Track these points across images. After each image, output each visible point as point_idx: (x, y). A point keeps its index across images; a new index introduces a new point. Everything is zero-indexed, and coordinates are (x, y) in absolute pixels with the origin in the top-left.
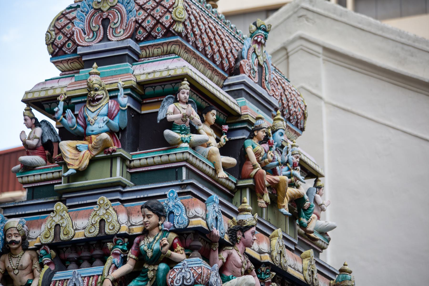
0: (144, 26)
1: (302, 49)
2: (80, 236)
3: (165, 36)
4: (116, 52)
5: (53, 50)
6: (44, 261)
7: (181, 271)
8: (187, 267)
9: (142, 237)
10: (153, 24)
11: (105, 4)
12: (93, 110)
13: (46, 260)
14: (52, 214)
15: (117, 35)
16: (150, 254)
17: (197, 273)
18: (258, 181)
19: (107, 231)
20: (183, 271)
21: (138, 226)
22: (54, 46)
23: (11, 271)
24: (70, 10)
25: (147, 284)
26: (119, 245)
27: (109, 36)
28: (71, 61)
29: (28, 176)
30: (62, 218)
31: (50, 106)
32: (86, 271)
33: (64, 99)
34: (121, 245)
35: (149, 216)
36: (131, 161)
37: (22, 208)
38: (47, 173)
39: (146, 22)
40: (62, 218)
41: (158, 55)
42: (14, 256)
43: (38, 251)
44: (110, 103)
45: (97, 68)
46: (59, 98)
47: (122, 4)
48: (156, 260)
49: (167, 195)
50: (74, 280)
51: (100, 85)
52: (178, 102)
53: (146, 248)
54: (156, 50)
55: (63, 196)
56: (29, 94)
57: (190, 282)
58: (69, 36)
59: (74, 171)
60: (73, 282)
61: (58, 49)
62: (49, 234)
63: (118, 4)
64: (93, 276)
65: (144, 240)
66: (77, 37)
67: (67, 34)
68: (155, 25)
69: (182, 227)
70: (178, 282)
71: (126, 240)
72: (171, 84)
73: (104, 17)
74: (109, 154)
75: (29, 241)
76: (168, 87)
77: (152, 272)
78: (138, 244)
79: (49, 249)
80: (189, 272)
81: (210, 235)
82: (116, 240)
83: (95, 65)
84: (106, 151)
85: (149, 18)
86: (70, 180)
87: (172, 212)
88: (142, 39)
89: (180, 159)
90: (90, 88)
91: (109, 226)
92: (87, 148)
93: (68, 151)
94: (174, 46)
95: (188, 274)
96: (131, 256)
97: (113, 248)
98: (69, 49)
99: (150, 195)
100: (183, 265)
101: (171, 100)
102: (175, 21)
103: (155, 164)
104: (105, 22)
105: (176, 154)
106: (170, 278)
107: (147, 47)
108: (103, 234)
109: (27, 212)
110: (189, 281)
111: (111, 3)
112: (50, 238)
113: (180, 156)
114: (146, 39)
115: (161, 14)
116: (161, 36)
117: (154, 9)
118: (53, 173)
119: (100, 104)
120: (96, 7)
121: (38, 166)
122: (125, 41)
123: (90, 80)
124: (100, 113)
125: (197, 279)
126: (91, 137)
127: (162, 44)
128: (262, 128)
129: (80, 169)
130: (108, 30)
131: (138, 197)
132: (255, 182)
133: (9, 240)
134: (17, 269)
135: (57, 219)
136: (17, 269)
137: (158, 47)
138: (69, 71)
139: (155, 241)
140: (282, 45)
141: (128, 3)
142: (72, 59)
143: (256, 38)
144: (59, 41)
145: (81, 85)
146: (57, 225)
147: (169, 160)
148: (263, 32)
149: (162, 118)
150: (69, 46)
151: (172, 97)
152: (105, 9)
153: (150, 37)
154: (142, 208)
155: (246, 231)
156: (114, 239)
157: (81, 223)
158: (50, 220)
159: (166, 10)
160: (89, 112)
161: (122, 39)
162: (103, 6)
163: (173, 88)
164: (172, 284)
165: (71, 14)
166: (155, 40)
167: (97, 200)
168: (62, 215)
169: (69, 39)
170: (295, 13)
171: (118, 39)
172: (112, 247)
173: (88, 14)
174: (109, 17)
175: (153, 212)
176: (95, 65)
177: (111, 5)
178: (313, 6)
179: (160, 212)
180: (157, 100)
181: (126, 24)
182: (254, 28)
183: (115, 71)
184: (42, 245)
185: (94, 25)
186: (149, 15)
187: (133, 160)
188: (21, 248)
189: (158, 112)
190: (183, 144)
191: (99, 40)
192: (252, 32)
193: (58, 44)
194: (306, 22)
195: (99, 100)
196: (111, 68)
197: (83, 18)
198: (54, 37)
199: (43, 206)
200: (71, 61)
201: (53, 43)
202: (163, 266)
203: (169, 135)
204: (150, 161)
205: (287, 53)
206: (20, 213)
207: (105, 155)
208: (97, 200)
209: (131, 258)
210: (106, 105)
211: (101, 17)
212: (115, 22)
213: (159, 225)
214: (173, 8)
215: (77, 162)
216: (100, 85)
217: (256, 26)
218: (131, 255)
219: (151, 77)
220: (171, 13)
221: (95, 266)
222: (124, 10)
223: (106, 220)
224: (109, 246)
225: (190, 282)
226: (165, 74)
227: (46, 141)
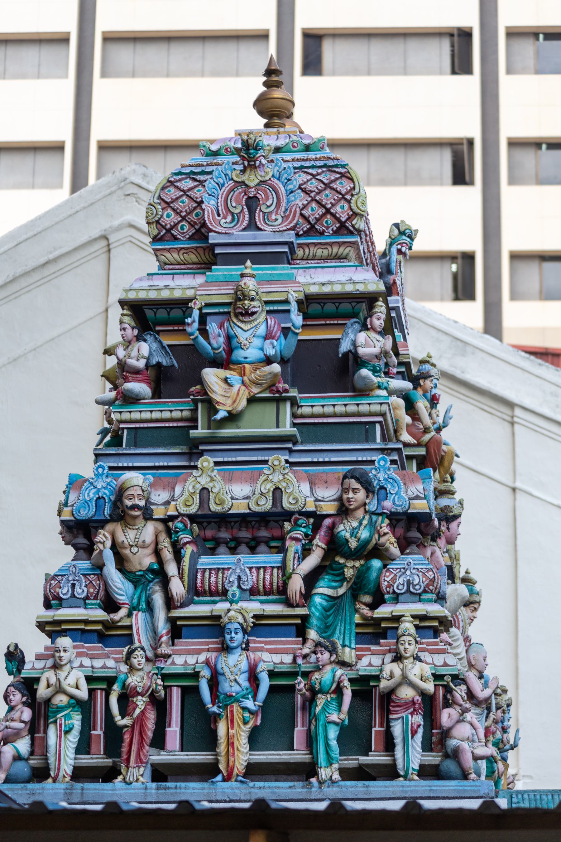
0: (307, 215)
1: (130, 241)
2: (240, 508)
3: (336, 233)
4: (268, 247)
5: (157, 231)
6: (182, 539)
7: (405, 572)
8: (414, 569)
9: (337, 519)
10: (321, 213)
11: (252, 177)
12: (246, 328)
13: (185, 537)
14: (195, 472)
15: (271, 223)
16: (353, 544)
17: (428, 578)
18: (432, 451)
19: (286, 505)
20: (408, 573)
21: (329, 503)
22: (158, 226)
23: (125, 548)
24: (180, 177)
25: (341, 586)
26: (301, 526)
27: (258, 223)
28: (185, 251)
29: (130, 412)
30: (212, 480)
31: (155, 313)
32: (246, 559)
33: (200, 306)
34: (304, 527)
35: (355, 491)
36: (299, 407)
37: (128, 458)
38: (161, 411)
39: (310, 209)
40: (212, 480)
41: (322, 259)
42: (131, 527)
43: (170, 524)
44: (269, 320)
45: (251, 267)
46: (193, 305)
47: (279, 179)
48: (359, 554)
49: (376, 462)
50: (238, 571)
51: (257, 294)
52: (368, 329)
53: (348, 535)
54: (320, 251)
55: (201, 448)
56: (130, 292)
57: (419, 589)
58: (183, 214)
59: (226, 414)
60: (237, 574)
61: (164, 231)
62: (191, 500)
63: (272, 179)
64: (264, 568)
65: (342, 523)
66: (209, 218)
67: (181, 211)
68: (324, 215)
69: (400, 510)
70: (400, 587)
71: (312, 520)
72: (350, 303)
73: (251, 195)
74: (277, 395)
75: (153, 507)
76: (345, 307)
77: (351, 570)
78: (332, 527)
79: (189, 523)
80: (418, 575)
81: (427, 526)
82: (297, 520)
83: (249, 263)
84: (273, 390)
85: (314, 205)
86: (212, 425)
87: (382, 488)
88: (301, 232)
89: (375, 412)
90: (240, 295)
91: (288, 498)
92: (241, 382)
93: (216, 383)
94: (349, 248)
95: (416, 578)
96: (320, 544)
97: (290, 531)
98: (183, 233)
99: (333, 459)
100: (408, 564)
101: (357, 326)
102: (355, 214)
103: (335, 415)
104: (252, 203)
105: (369, 404)
106: (385, 580)
107: (308, 245)
108: (279, 510)
109: (136, 464)
110: (417, 587)
111: (261, 176)
112: (193, 506)
113: (375, 408)
114: (307, 233)
115: (333, 202)
116: (331, 232)
117: (320, 192)
118: (171, 411)
119: (255, 320)
120: (238, 180)
121: (144, 399)
122: (286, 233)
123: (245, 284)
124: (257, 333)
125: (427, 586)
126: (244, 367)
127: (331, 244)
128: (430, 376)
129: (234, 412)
130: (257, 215)
131: (315, 460)
132: (427, 451)
133: (128, 503)
134: (136, 545)
135: (204, 481)
136: (136, 545)
137: (325, 247)
138: (179, 264)
139: (363, 527)
140: (103, 233)
141: (289, 180)
142: (188, 248)
143: (399, 247)
144: (167, 219)
145: (220, 289)
146: (204, 489)
147: (358, 412)
148: (408, 240)
149: (345, 350)
150: (182, 228)
151: (358, 322)
152: (252, 184)
153: (312, 231)
154: (345, 477)
155: (452, 521)
156: (293, 518)
157: (241, 489)
158: (193, 481)
159: (340, 196)
160: (239, 330)
161: (281, 229)
162: (249, 180)
163: (353, 308)
164: (388, 589)
165: (183, 182)
166: (322, 237)
167: (270, 459)
168: (213, 475)
169: (184, 218)
170: (121, 188)
171: (274, 230)
172: (289, 528)
173: (224, 188)
174: (258, 195)
175: (362, 486)
176: (249, 263)
177: (262, 179)
178: (148, 183)
179: (367, 486)
180: (323, 322)
181: (286, 210)
182: (396, 232)
183: (271, 275)
184: (181, 515)
185: (234, 204)
186: (314, 199)
187: (302, 406)
188: (141, 516)
189: (339, 339)
190: (381, 391)
191: (243, 227)
192: (393, 237)
193: (166, 225)
194: (136, 204)
195: (253, 313)
196: (262, 269)
197: (216, 192)
198: (161, 213)
199: (161, 458)
200: (185, 251)
201: (158, 222)
202: (376, 563)
203: (364, 378)
204: (329, 410)
205: (109, 245)
206: (125, 465)
207: (272, 395)
208: (270, 459)
209: (319, 546)
210: (261, 323)
211: (245, 194)
212: (269, 203)
213: (365, 504)
214: (352, 195)
215: (229, 402)
216: (257, 294)
217: (399, 230)
218: (319, 542)
219: (327, 289)
220: (349, 202)
221: (262, 553)
222: (282, 190)
223: (283, 489)
224: (286, 526)
225: (419, 589)
226: (349, 288)
227: (154, 363)
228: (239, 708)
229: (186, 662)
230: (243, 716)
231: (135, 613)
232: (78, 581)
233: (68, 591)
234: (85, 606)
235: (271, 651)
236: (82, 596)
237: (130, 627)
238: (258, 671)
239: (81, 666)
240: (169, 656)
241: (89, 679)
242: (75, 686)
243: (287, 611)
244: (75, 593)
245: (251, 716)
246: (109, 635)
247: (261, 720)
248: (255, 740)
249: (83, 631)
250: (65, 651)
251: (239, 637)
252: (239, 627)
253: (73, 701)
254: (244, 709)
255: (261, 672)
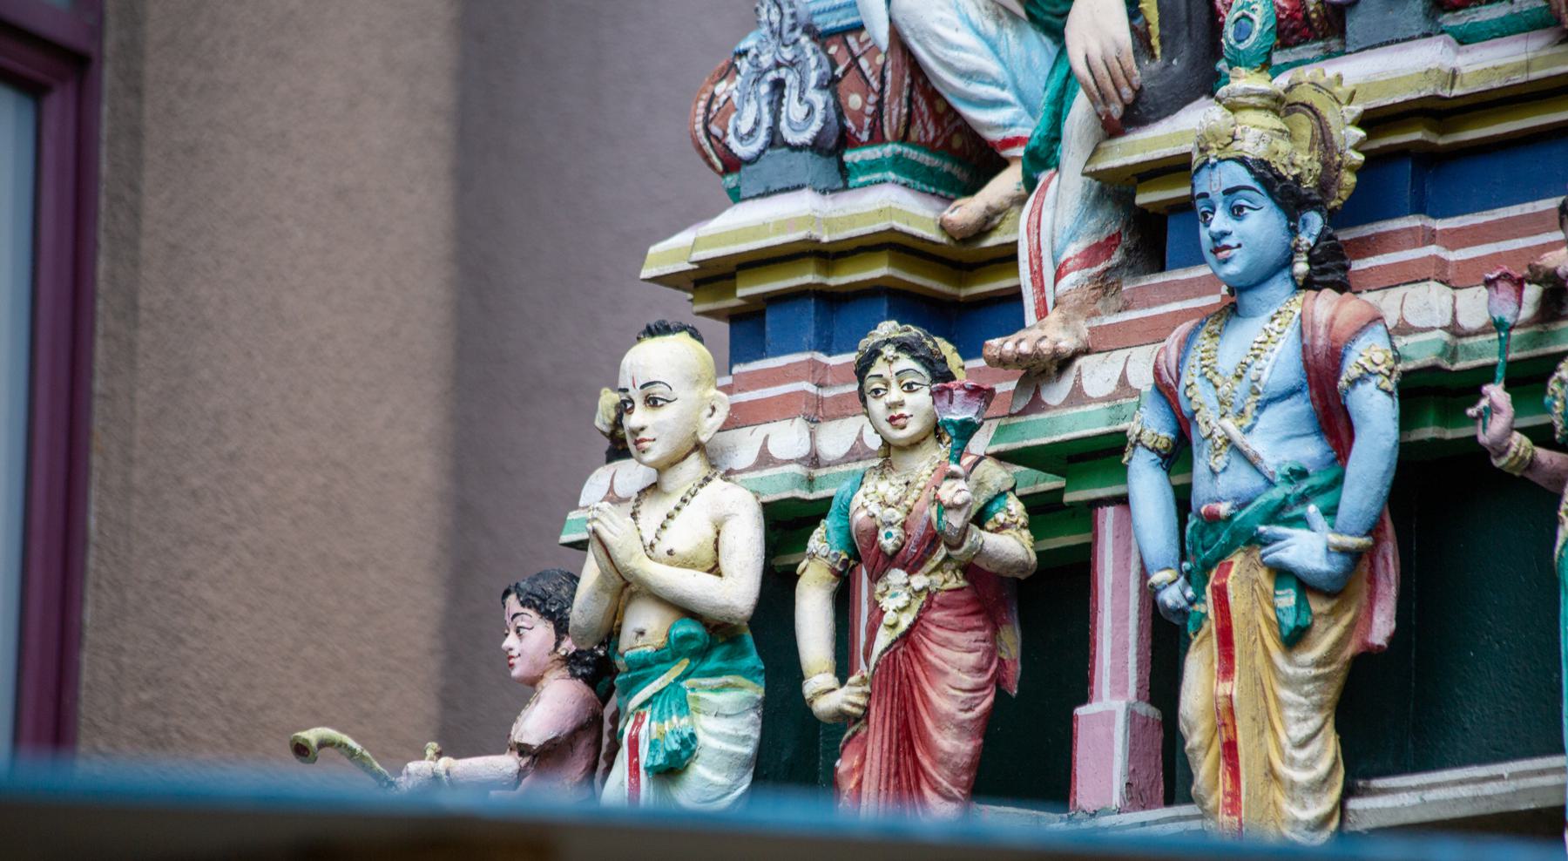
228: (1263, 574)
229: (1123, 381)
230: (1275, 608)
231: (1043, 177)
232: (792, 64)
233: (757, 123)
234: (843, 179)
235: (1450, 277)
236: (806, 137)
237: (1007, 257)
238: (1343, 383)
239: (765, 459)
240: (1063, 363)
241: (787, 525)
242: (707, 554)
243: (1549, 62)
244: (783, 124)
245: (1318, 606)
246: (956, 294)
247: (1401, 615)
248: (1382, 716)
249: (830, 301)
250: (652, 402)
251: (1260, 226)
252: (1245, 178)
253: (687, 628)
254: (1281, 573)
255: (1353, 383)
